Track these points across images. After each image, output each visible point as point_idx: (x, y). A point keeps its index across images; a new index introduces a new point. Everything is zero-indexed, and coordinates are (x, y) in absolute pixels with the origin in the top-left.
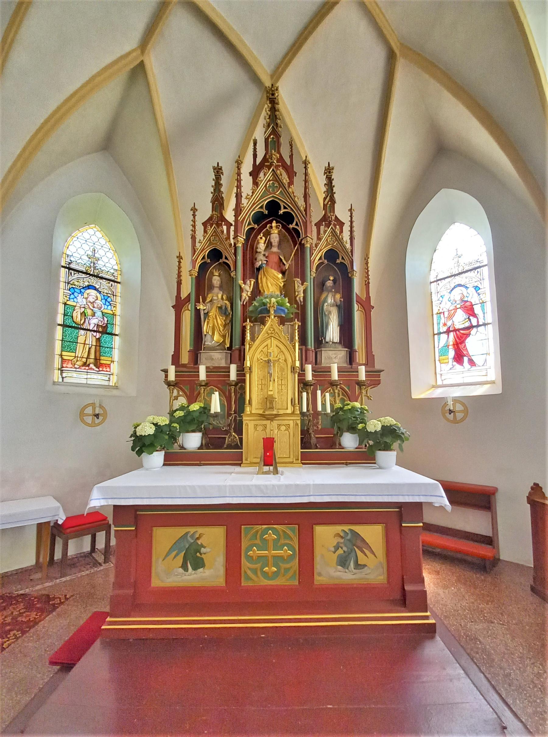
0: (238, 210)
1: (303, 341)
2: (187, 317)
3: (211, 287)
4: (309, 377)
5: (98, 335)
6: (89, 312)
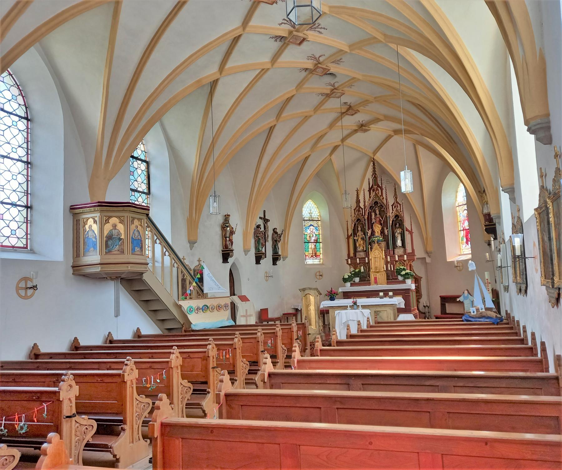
2: (351, 241)
4: (389, 260)
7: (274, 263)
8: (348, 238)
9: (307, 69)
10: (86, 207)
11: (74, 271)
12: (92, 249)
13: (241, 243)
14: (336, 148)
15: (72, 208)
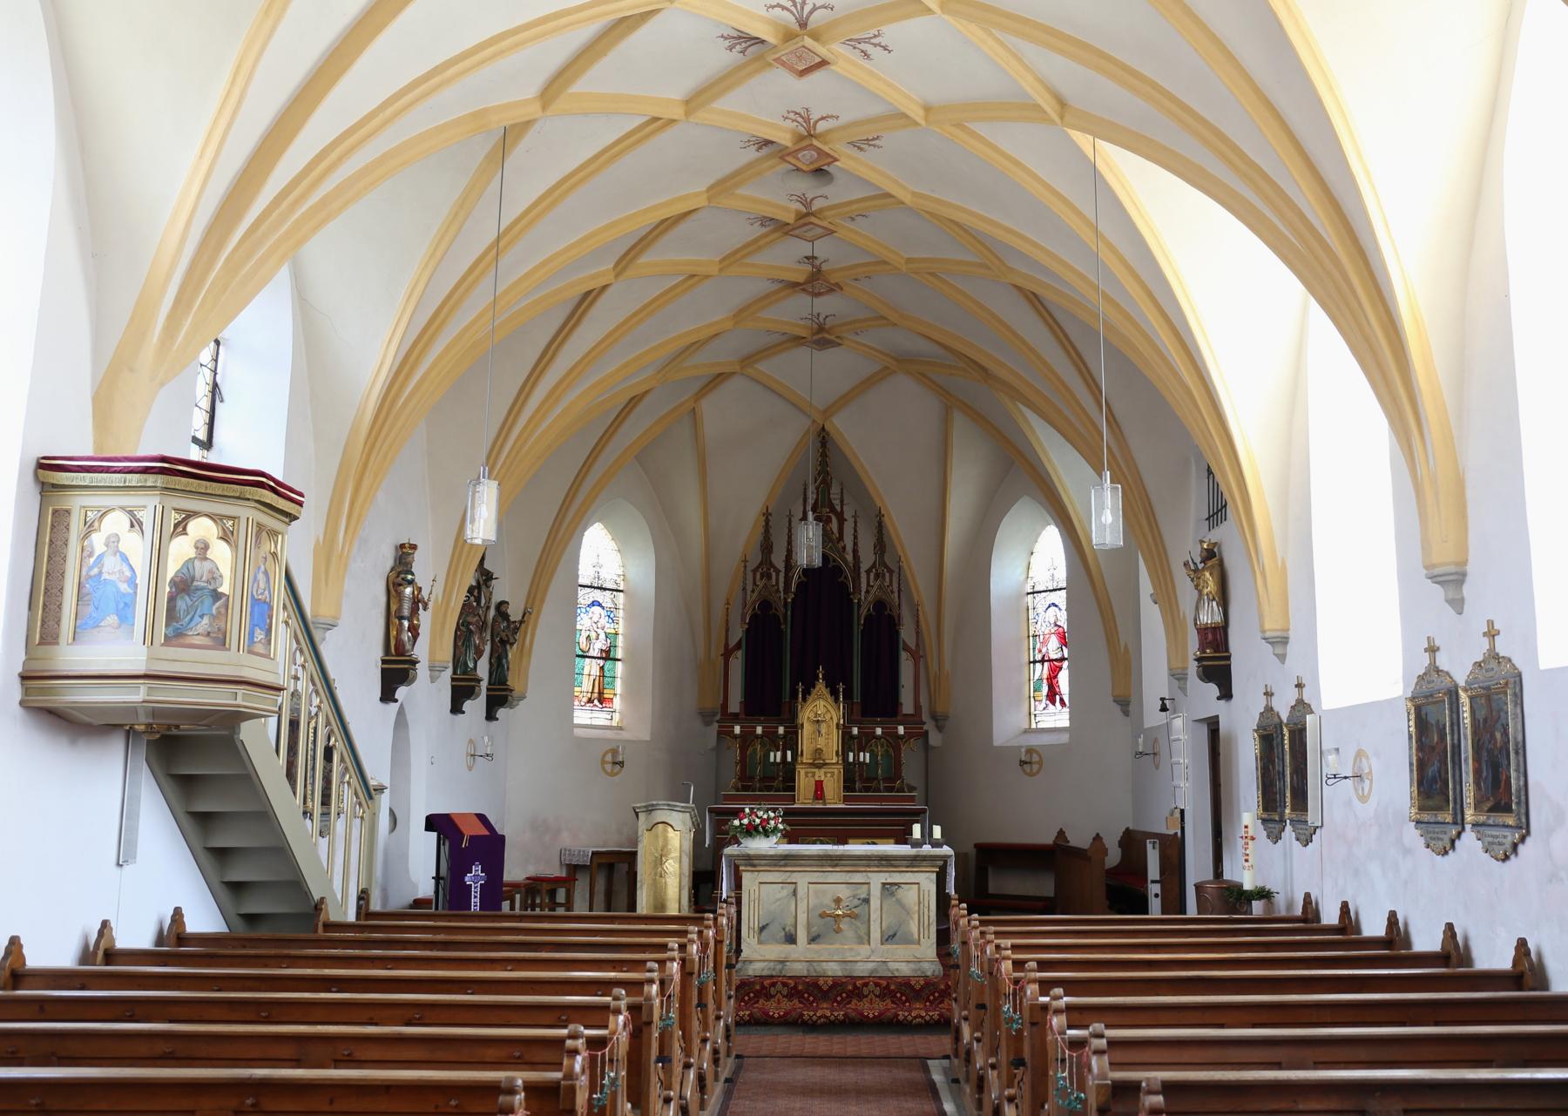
5: (601, 662)
6: (593, 635)
7: (491, 716)
8: (727, 654)
9: (768, 143)
10: (107, 470)
11: (26, 691)
12: (112, 619)
13: (432, 645)
14: (719, 378)
15: (46, 465)
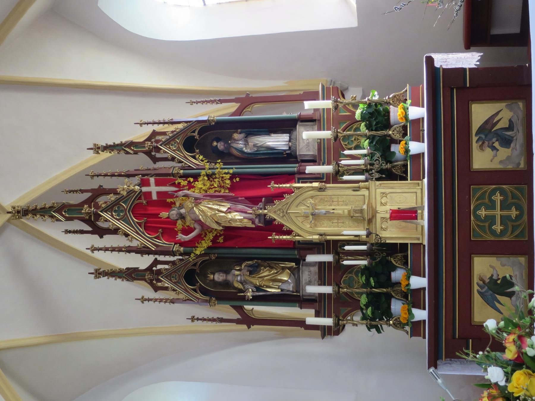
0: (143, 251)
1: (289, 177)
3: (227, 284)
4: (327, 169)
8: (248, 320)
